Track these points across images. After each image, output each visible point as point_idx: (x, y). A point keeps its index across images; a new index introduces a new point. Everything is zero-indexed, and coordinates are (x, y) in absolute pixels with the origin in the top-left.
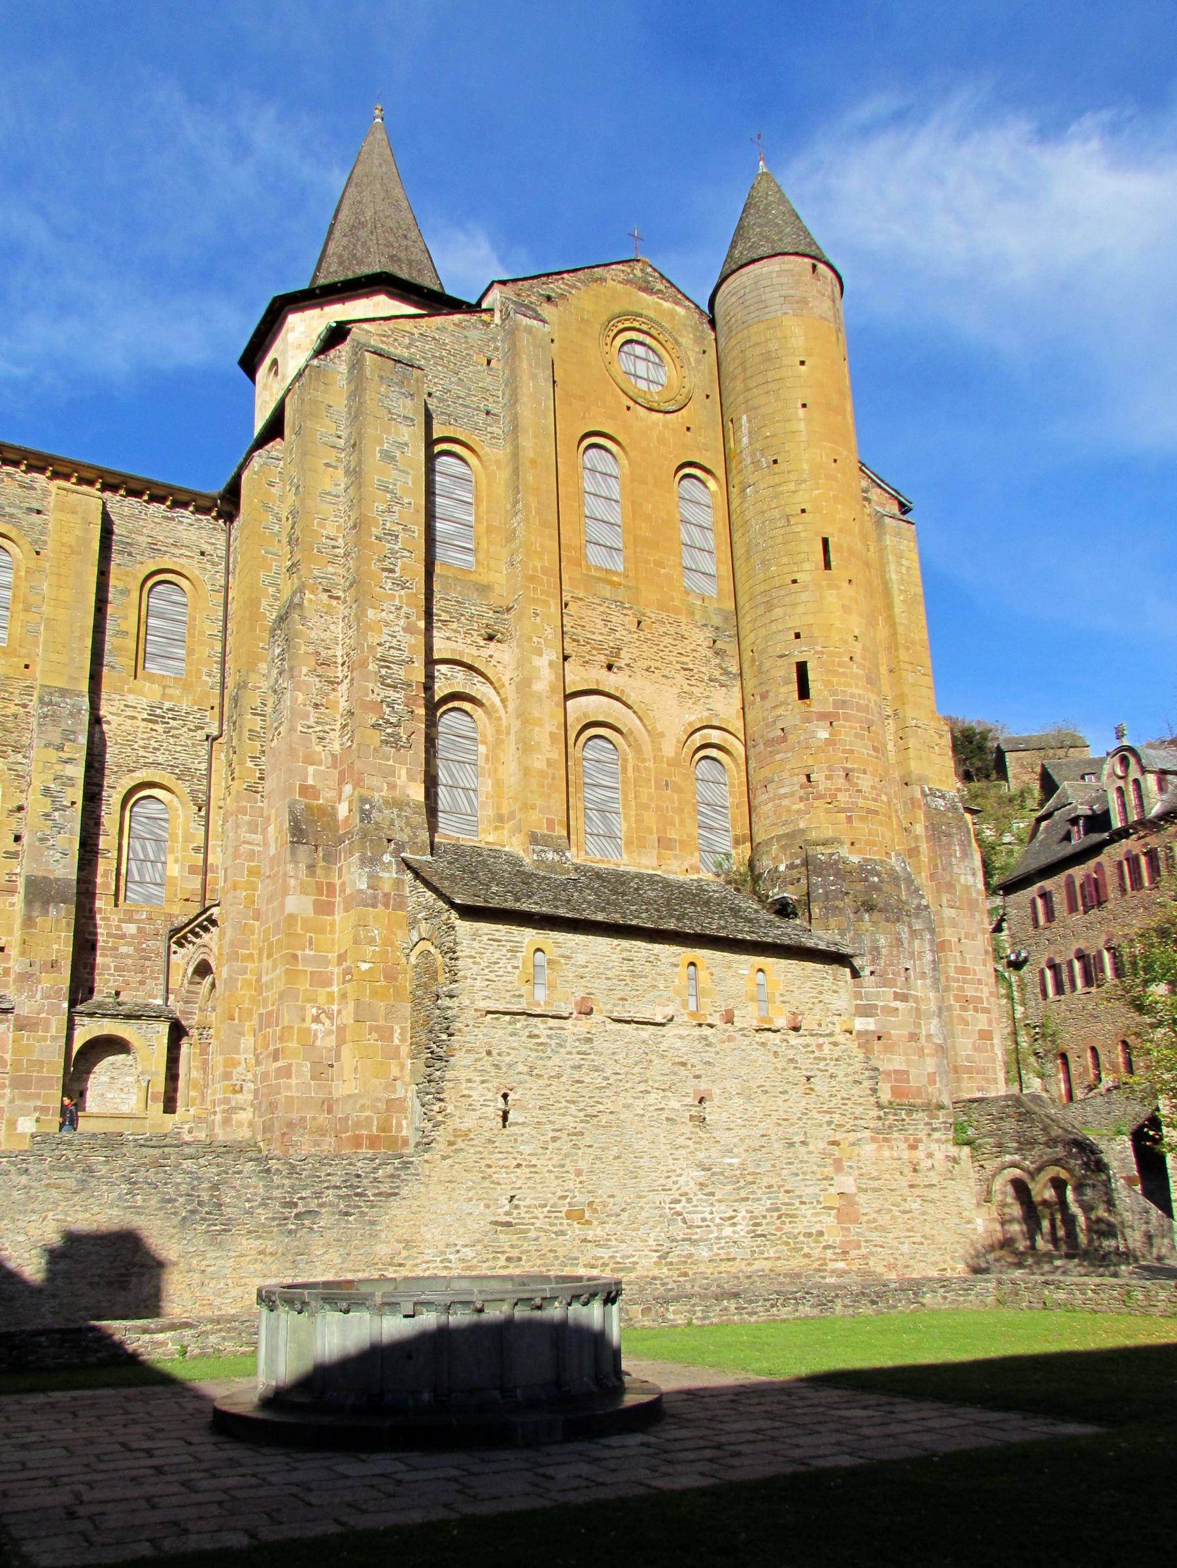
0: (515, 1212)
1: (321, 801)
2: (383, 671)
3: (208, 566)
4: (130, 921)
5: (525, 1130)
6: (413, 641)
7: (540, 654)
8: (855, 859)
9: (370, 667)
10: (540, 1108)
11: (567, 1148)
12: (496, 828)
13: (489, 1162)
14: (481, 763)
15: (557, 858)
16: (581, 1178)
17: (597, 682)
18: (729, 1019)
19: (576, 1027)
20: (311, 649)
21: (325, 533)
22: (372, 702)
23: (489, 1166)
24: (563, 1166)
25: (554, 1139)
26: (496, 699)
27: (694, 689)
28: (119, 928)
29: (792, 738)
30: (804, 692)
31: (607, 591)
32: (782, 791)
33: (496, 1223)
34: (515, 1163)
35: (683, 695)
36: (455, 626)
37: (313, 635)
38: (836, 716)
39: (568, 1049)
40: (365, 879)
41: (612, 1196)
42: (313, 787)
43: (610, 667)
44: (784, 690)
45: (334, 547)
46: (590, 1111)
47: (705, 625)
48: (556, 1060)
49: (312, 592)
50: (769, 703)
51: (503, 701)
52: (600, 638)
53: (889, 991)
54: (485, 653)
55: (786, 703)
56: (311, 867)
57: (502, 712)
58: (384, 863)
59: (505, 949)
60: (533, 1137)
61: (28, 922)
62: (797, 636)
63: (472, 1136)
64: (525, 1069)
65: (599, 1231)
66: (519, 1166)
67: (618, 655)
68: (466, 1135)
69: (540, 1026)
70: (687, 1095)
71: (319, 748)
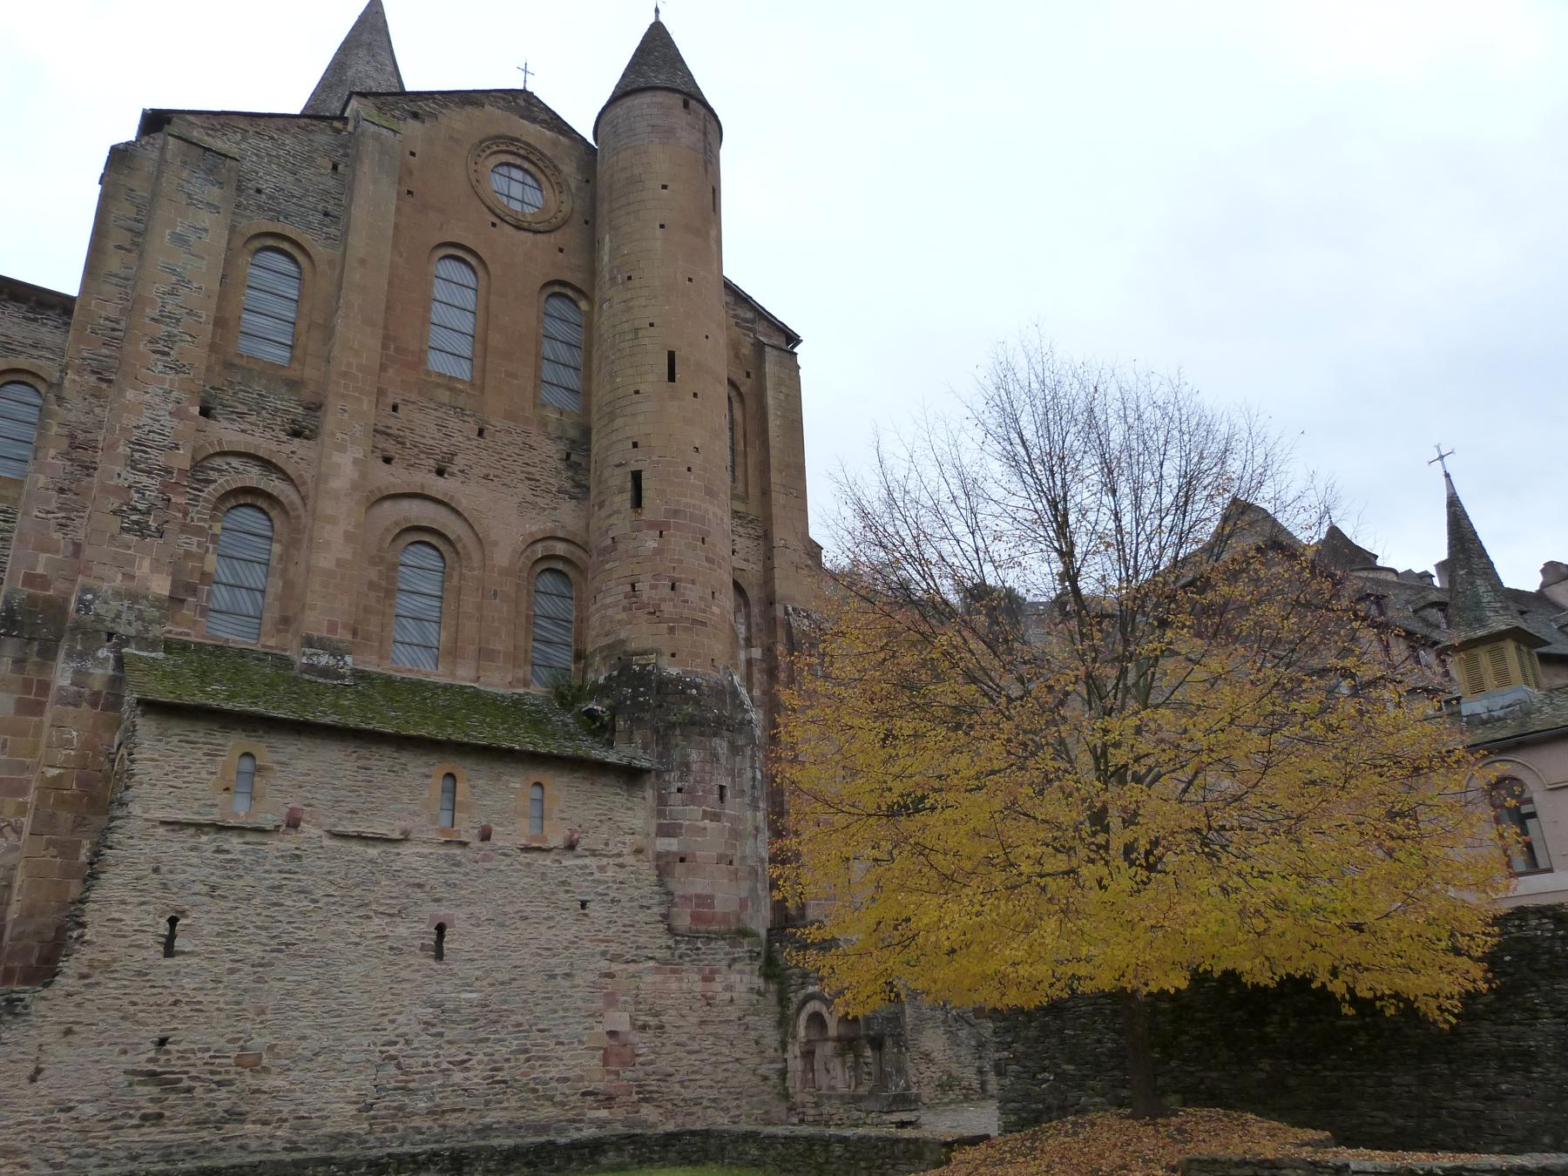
0: (164, 1058)
1: (51, 592)
2: (137, 455)
5: (195, 960)
6: (180, 427)
7: (342, 449)
8: (674, 671)
9: (121, 449)
10: (218, 934)
11: (247, 982)
12: (279, 631)
13: (135, 999)
14: (274, 563)
15: (332, 662)
16: (263, 1017)
17: (422, 487)
18: (486, 835)
19: (287, 843)
20: (65, 431)
21: (104, 314)
22: (117, 486)
23: (135, 1004)
24: (238, 1003)
25: (232, 971)
26: (295, 497)
27: (538, 500)
29: (621, 546)
30: (637, 502)
31: (444, 396)
32: (608, 601)
33: (134, 1073)
34: (173, 999)
35: (524, 505)
36: (253, 418)
37: (72, 417)
38: (668, 525)
39: (267, 867)
40: (69, 674)
41: (304, 1038)
42: (42, 576)
44: (618, 499)
45: (113, 330)
46: (285, 938)
47: (560, 438)
48: (249, 880)
49: (78, 373)
50: (604, 512)
51: (303, 499)
52: (432, 442)
53: (697, 811)
54: (287, 448)
55: (618, 512)
56: (19, 663)
57: (301, 511)
58: (96, 658)
59: (200, 753)
60: (202, 968)
62: (635, 445)
63: (116, 966)
64: (205, 889)
65: (280, 1082)
66: (176, 1003)
67: (451, 461)
68: (107, 967)
69: (234, 842)
70: (421, 921)
71: (58, 536)
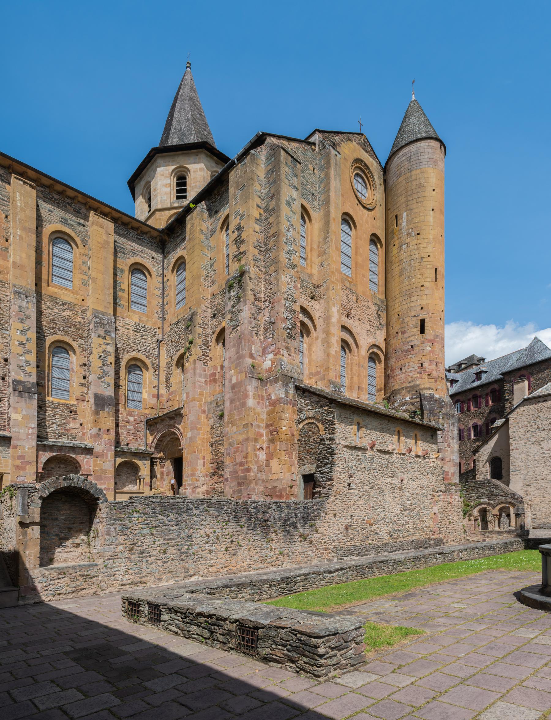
3: (155, 264)
4: (131, 415)
12: (311, 378)
14: (305, 351)
28: (127, 418)
43: (348, 317)
61: (97, 413)
